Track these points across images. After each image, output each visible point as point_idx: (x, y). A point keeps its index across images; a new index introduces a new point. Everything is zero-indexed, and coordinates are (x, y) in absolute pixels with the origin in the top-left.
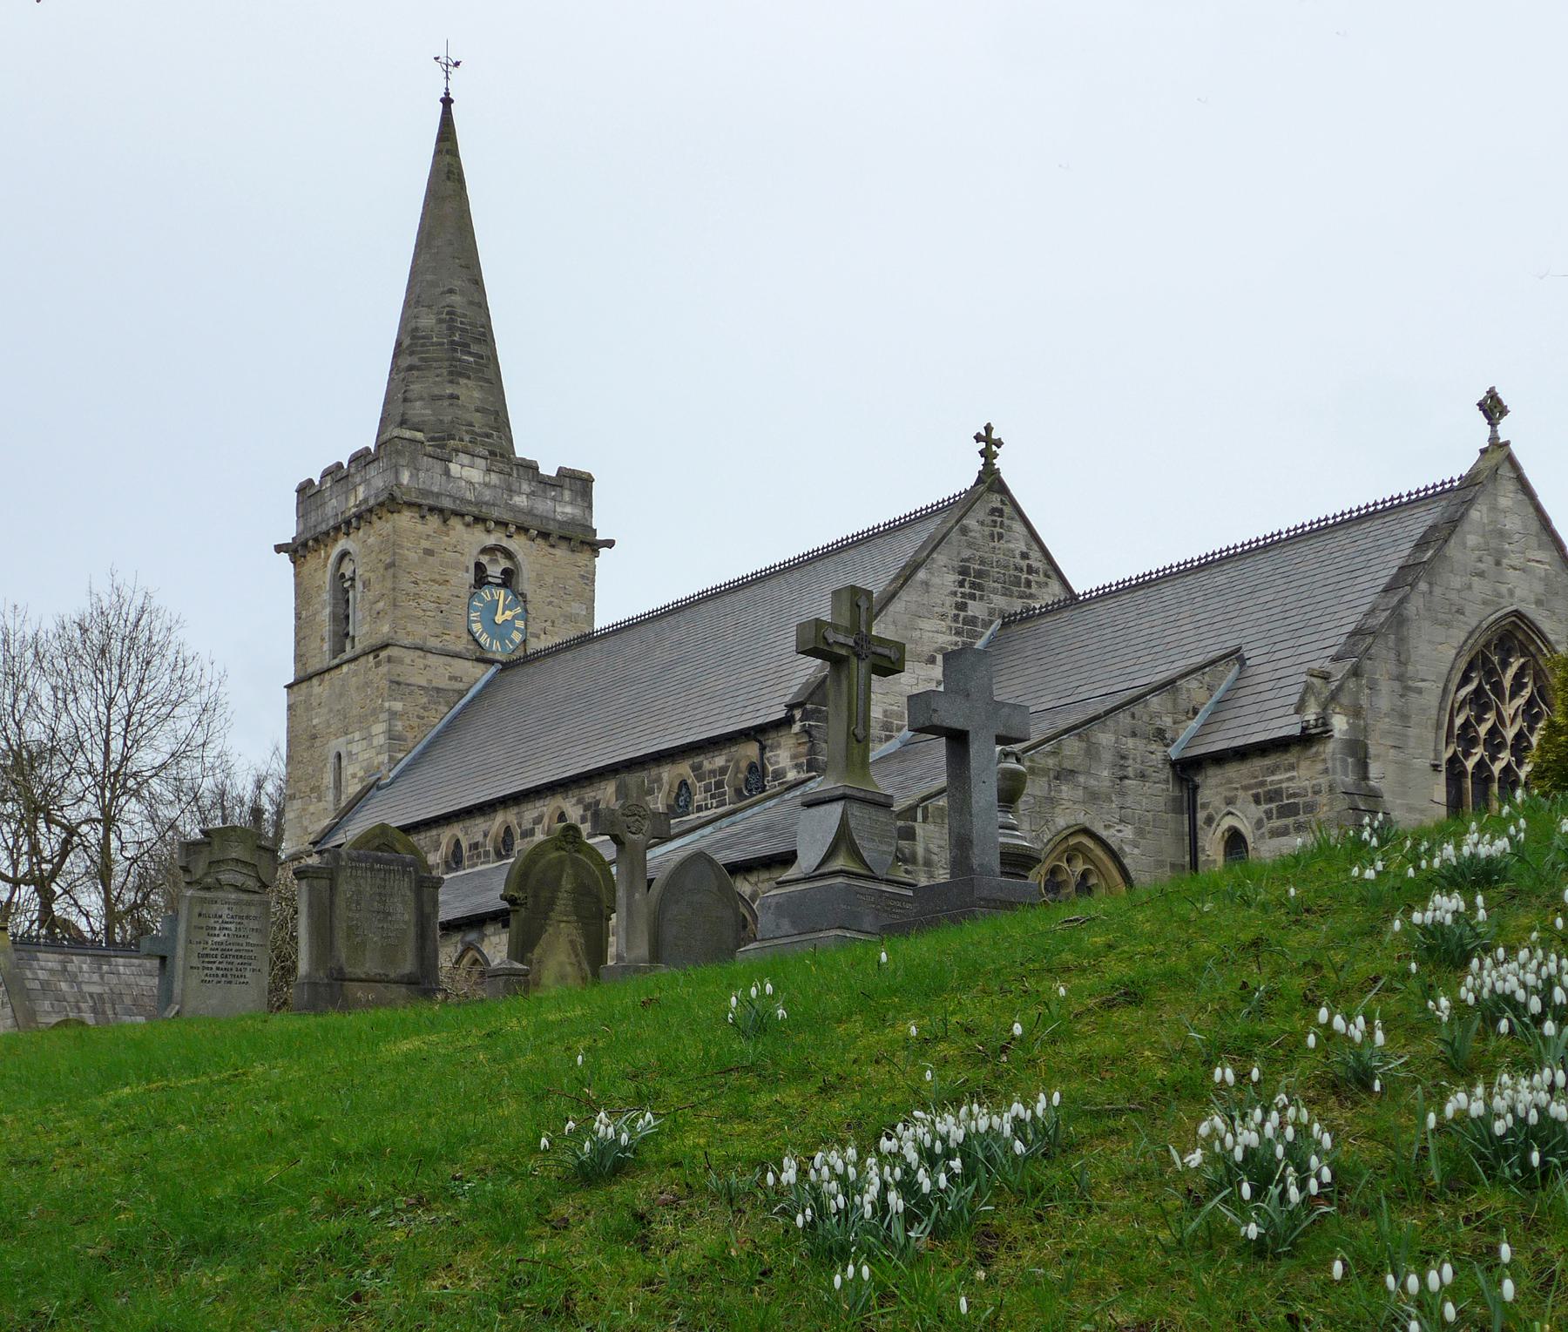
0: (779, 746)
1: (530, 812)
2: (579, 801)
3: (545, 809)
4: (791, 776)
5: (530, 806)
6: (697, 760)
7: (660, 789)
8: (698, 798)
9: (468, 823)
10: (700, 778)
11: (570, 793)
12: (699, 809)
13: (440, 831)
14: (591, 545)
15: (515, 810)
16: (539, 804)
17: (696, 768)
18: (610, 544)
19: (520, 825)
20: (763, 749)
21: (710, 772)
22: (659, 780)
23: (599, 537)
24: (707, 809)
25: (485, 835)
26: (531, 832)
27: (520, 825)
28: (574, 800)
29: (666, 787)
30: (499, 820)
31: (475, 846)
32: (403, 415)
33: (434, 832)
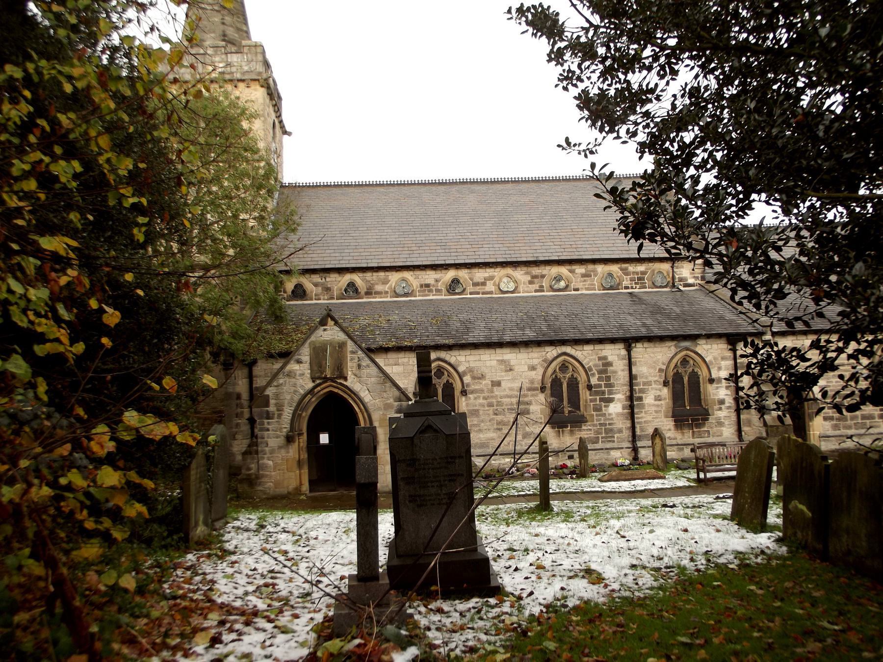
0: (683, 267)
1: (480, 274)
2: (527, 273)
3: (496, 274)
4: (691, 281)
5: (480, 270)
6: (624, 266)
7: (595, 275)
8: (625, 283)
9: (418, 273)
10: (627, 274)
11: (519, 269)
12: (626, 288)
13: (387, 273)
14: (285, 132)
15: (466, 271)
16: (488, 270)
17: (621, 269)
18: (289, 134)
19: (471, 279)
20: (672, 267)
21: (634, 273)
22: (595, 271)
23: (288, 129)
24: (632, 288)
25: (437, 281)
26: (484, 284)
27: (471, 279)
28: (522, 272)
29: (600, 275)
30: (451, 274)
31: (428, 286)
32: (224, 31)
33: (382, 274)
